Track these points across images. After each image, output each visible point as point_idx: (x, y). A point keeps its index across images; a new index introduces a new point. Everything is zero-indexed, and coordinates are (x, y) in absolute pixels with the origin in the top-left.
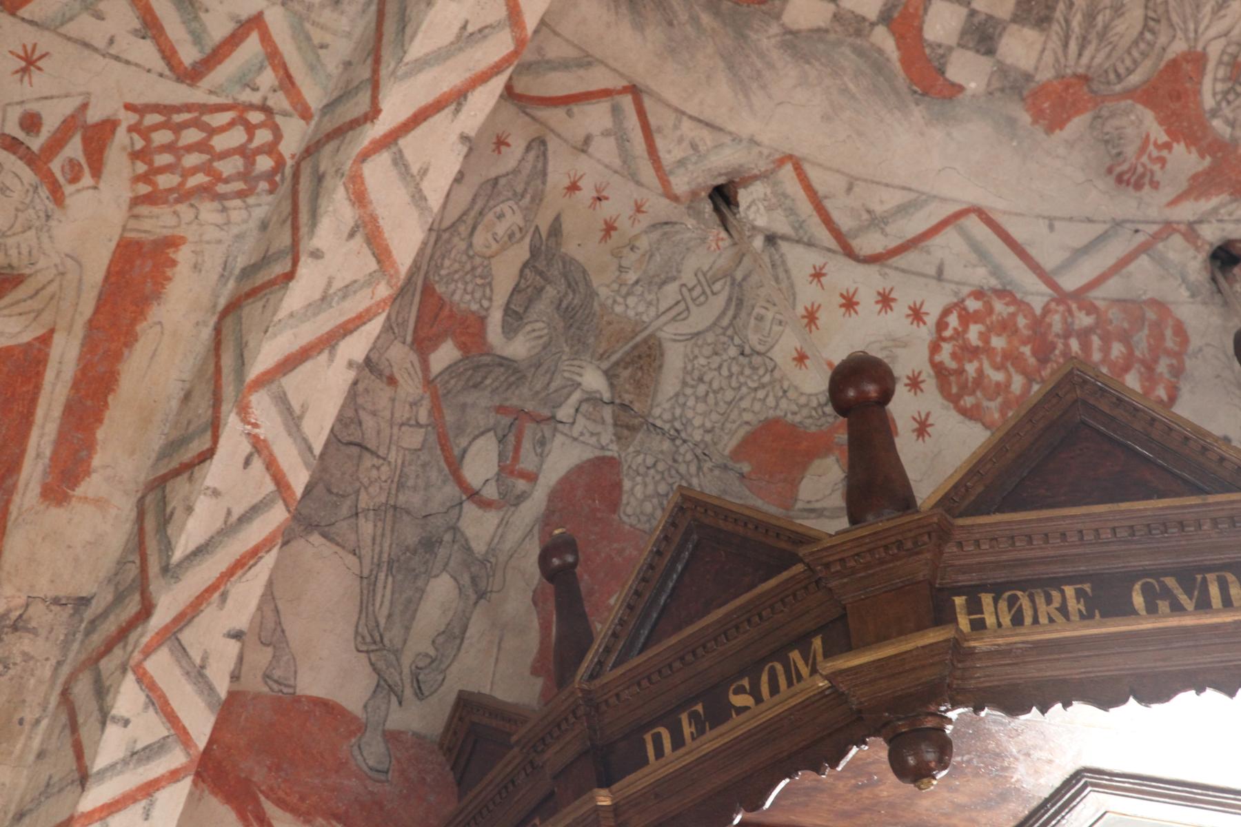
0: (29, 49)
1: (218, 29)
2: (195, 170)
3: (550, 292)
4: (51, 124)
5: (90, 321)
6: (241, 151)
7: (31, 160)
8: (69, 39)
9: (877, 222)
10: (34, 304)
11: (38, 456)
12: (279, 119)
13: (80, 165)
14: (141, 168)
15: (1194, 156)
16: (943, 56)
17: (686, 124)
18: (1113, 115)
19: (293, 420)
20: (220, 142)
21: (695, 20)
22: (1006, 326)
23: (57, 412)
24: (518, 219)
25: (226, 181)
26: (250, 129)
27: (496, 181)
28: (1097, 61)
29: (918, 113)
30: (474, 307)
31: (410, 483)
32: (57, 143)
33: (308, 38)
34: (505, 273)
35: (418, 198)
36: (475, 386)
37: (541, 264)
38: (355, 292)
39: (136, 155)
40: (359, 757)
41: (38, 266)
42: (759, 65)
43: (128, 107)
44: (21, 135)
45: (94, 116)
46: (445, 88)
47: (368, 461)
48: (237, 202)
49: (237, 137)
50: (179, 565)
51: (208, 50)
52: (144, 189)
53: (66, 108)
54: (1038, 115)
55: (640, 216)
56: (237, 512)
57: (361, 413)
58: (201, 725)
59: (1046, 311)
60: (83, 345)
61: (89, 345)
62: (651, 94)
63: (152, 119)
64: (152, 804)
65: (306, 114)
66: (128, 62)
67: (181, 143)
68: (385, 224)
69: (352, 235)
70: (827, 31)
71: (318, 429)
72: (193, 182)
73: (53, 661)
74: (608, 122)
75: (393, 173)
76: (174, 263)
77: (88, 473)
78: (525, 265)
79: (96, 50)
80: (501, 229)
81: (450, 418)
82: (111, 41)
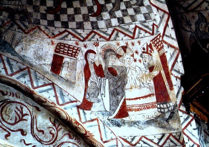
1: (151, 27)
4: (146, 48)
7: (147, 53)
10: (157, 68)
11: (167, 85)
35: (173, 38)
39: (155, 46)
43: (151, 41)
44: (144, 51)
45: (149, 44)
46: (164, 24)
52: (158, 49)
53: (146, 45)
61: (164, 70)
63: (154, 41)
64: (191, 124)
67: (158, 42)
68: (171, 43)
69: (168, 47)
75: (167, 38)
80: (203, 26)
82: (144, 35)
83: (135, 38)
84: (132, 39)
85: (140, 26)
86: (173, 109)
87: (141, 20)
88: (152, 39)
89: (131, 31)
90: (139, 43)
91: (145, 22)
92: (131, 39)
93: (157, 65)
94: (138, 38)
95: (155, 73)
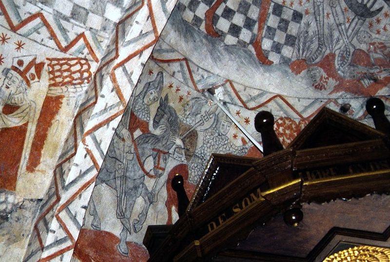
0: (20, 42)
1: (72, 37)
2: (66, 77)
3: (166, 116)
5: (38, 119)
6: (79, 71)
7: (22, 74)
8: (31, 39)
9: (253, 99)
10: (23, 114)
11: (25, 158)
12: (89, 62)
13: (34, 75)
14: (52, 76)
15: (334, 81)
16: (267, 53)
17: (200, 70)
18: (313, 70)
19: (98, 144)
20: (73, 69)
21: (201, 41)
22: (289, 127)
23: (30, 146)
24: (156, 95)
25: (76, 80)
26: (82, 65)
27: (149, 83)
28: (307, 55)
29: (261, 69)
30: (145, 119)
31: (130, 170)
32: (28, 68)
33: (97, 39)
34: (153, 109)
35: (130, 81)
36: (147, 142)
37: (163, 108)
38: (114, 108)
39: (50, 73)
40: (119, 250)
41: (23, 104)
42: (219, 54)
43: (47, 59)
44: (17, 66)
45: (38, 61)
47: (118, 162)
48: (79, 86)
49: (78, 67)
50: (67, 186)
51: (69, 43)
52: (52, 82)
53: (31, 59)
54: (293, 70)
55: (189, 96)
56: (83, 171)
57: (115, 148)
58: (75, 234)
59: (300, 123)
60: (37, 126)
61: (38, 126)
62: (190, 61)
63: (54, 62)
64: (63, 256)
65: (97, 61)
66: (47, 46)
67: (62, 69)
69: (112, 91)
70: (236, 45)
71: (105, 147)
72: (66, 80)
73: (32, 218)
74: (179, 69)
75: (123, 73)
76: (62, 103)
77: (39, 163)
78: (158, 108)
79: (38, 43)
81: (140, 152)
82: (42, 40)
83: (18, 32)
84: (12, 29)
85: (50, 20)
86: (7, 211)
87: (61, 11)
88: (54, 56)
89: (21, 15)
90: (20, 46)
91: (66, 19)
92: (9, 28)
93: (28, 110)
94: (26, 36)
95: (13, 121)
